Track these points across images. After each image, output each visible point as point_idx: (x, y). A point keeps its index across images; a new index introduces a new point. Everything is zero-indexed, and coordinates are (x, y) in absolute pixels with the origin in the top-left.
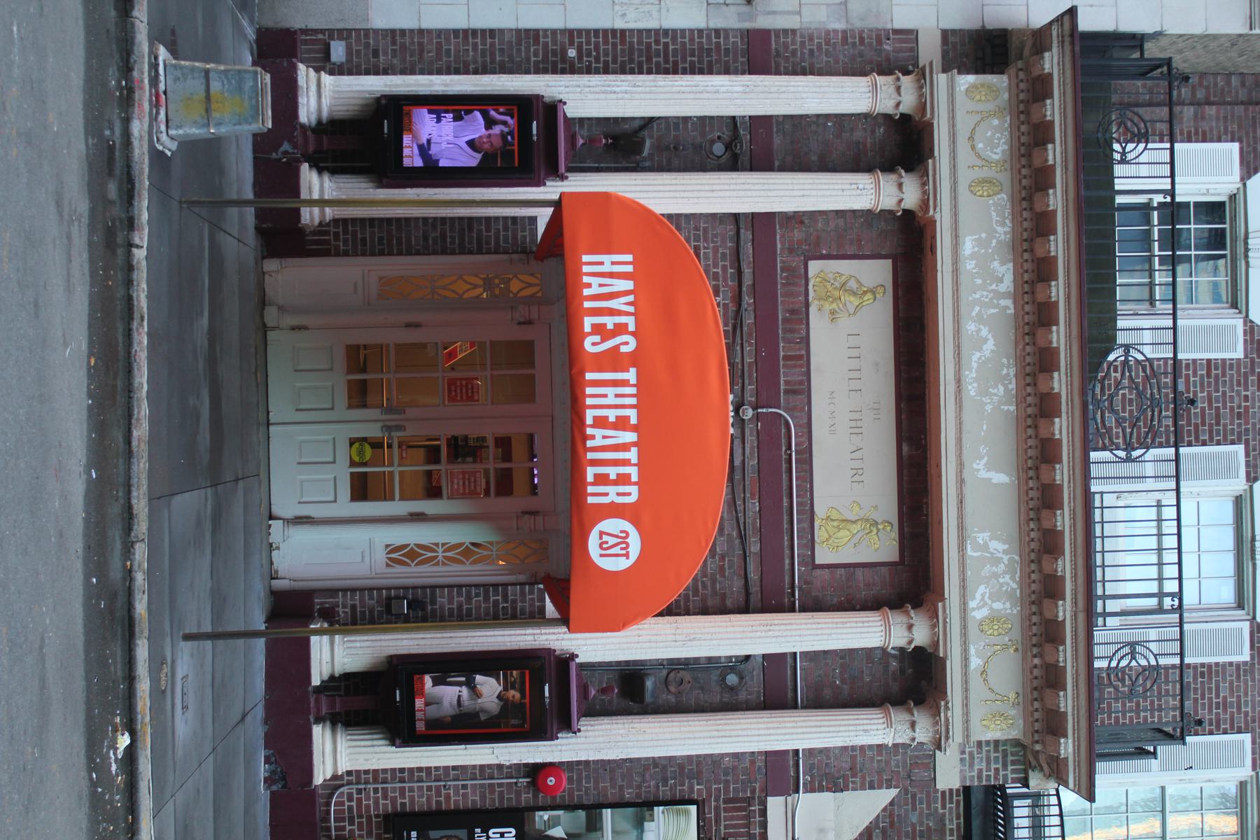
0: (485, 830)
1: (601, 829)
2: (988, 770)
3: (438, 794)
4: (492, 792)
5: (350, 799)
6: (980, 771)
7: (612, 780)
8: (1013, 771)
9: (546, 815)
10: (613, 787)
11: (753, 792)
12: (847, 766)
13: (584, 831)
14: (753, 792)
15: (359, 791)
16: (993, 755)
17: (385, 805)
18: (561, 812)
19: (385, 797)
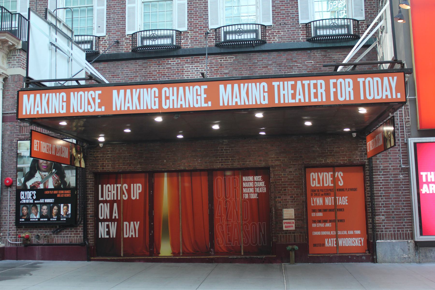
0: (21, 200)
1: (22, 168)
2: (16, 60)
3: (12, 213)
4: (12, 198)
5: (12, 238)
6: (17, 62)
7: (11, 165)
8: (17, 53)
9: (18, 183)
10: (13, 164)
11: (17, 125)
12: (12, 99)
13: (22, 173)
14: (17, 125)
15: (9, 235)
16: (13, 59)
17: (14, 228)
18: (17, 179)
19: (12, 228)
